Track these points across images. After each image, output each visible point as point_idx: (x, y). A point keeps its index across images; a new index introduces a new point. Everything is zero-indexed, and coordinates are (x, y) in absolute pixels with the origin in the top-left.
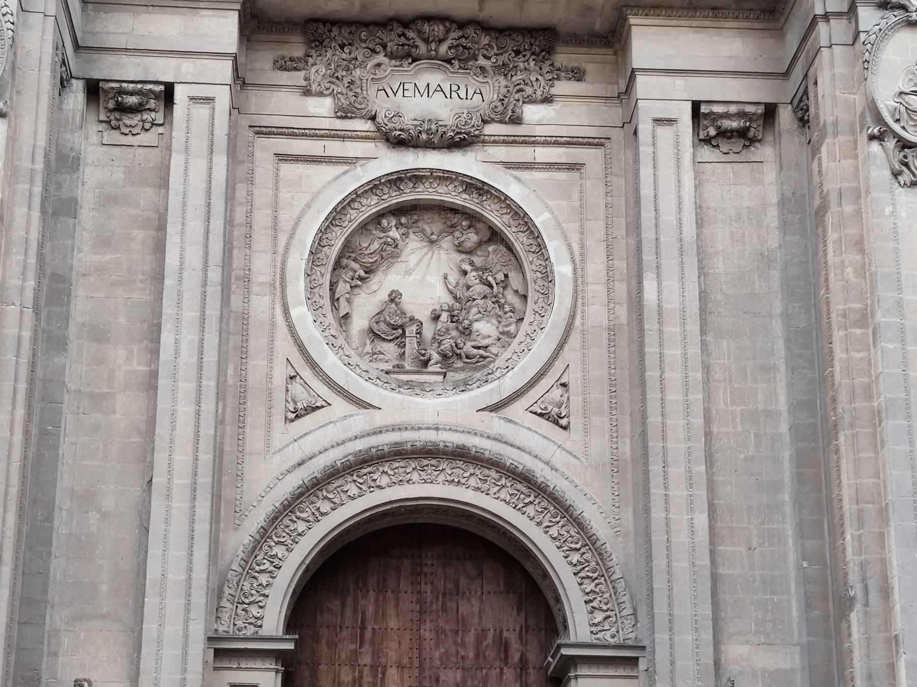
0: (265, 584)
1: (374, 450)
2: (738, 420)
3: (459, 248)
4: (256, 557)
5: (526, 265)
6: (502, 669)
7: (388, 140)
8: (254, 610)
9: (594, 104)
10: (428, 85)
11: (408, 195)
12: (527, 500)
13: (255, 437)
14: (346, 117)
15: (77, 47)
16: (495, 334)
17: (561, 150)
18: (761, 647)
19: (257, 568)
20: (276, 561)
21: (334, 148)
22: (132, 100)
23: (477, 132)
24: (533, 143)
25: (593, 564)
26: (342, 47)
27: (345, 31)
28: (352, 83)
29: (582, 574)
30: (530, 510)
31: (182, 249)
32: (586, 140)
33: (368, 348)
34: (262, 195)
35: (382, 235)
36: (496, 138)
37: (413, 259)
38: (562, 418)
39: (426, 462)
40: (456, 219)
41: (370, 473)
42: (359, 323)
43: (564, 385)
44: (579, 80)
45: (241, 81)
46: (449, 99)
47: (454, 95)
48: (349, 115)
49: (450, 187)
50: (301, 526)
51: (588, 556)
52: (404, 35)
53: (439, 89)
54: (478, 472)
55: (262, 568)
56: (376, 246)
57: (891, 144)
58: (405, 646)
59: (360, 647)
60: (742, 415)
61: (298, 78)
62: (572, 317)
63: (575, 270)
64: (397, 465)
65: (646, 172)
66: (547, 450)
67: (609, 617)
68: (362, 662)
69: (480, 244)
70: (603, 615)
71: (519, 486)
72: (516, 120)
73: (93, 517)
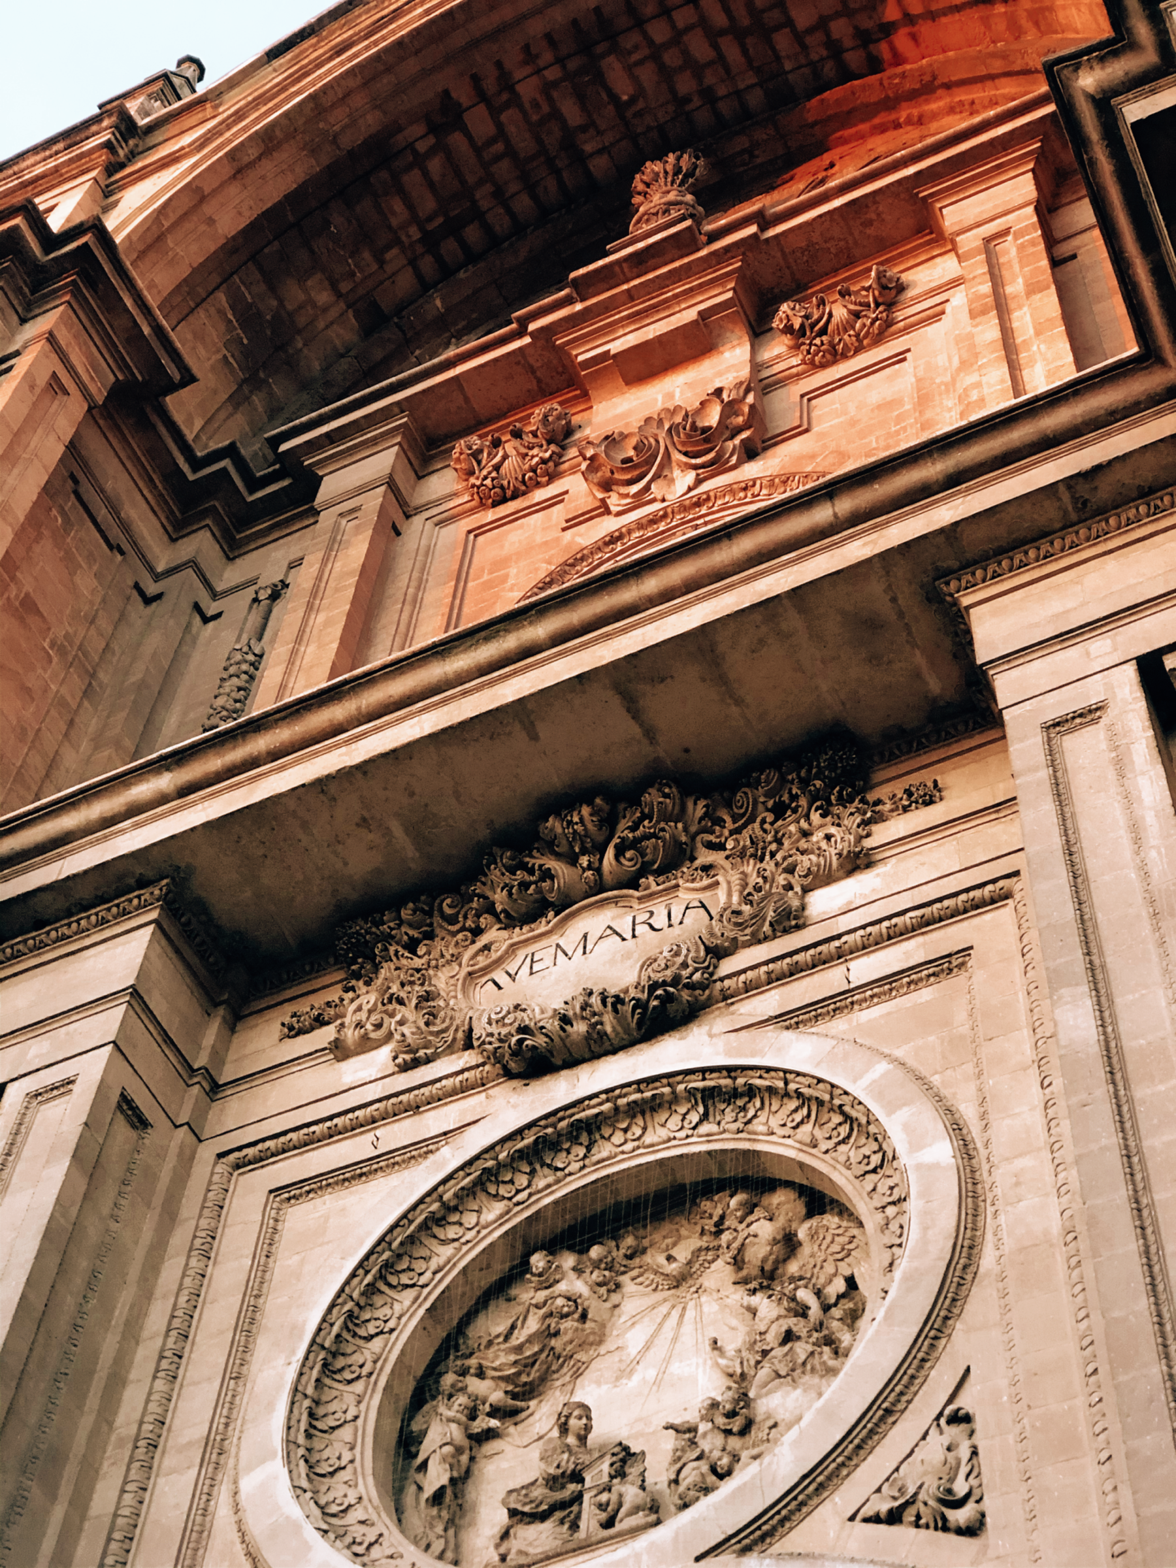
7: (509, 1075)
10: (585, 937)
14: (416, 1063)
23: (697, 976)
24: (841, 955)
28: (428, 997)
32: (963, 897)
35: (541, 1295)
36: (750, 974)
40: (713, 1207)
44: (929, 802)
46: (630, 942)
47: (640, 929)
48: (421, 1053)
49: (674, 1122)
52: (524, 867)
53: (609, 932)
56: (533, 1325)
61: (325, 1035)
69: (789, 1243)
72: (790, 920)
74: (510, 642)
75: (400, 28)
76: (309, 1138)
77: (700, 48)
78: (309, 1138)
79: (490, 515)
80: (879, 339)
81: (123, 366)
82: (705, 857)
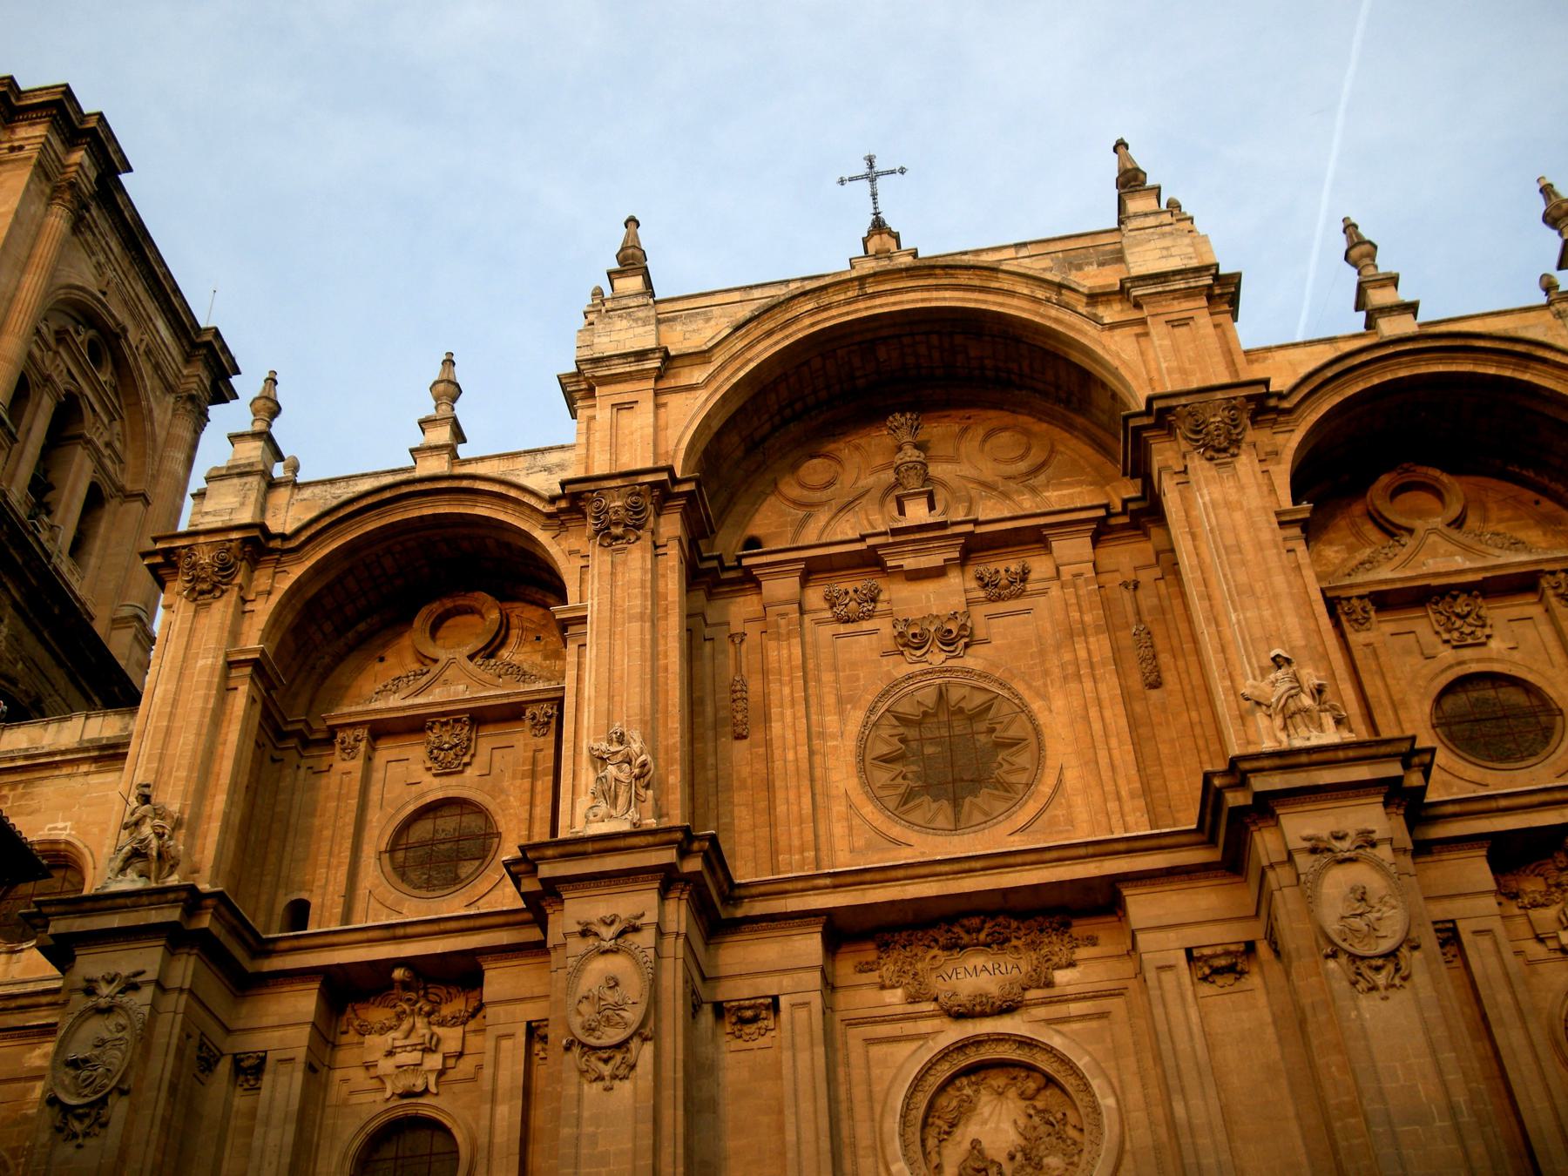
3: (1022, 1096)
5: (1078, 1103)
9: (1110, 963)
11: (974, 1057)
15: (704, 979)
17: (1089, 1003)
21: (909, 1028)
22: (749, 1013)
26: (904, 947)
27: (904, 935)
28: (915, 974)
31: (798, 1127)
34: (858, 1073)
37: (986, 1111)
40: (1015, 1072)
44: (1094, 945)
45: (830, 986)
56: (954, 1103)
57: (1343, 959)
61: (874, 977)
62: (1122, 1143)
63: (1118, 1101)
65: (1158, 1011)
69: (1039, 1090)
72: (1050, 984)
74: (966, 866)
75: (799, 330)
76: (873, 1021)
77: (923, 350)
78: (873, 1021)
79: (842, 628)
80: (1018, 596)
81: (692, 532)
82: (1014, 942)
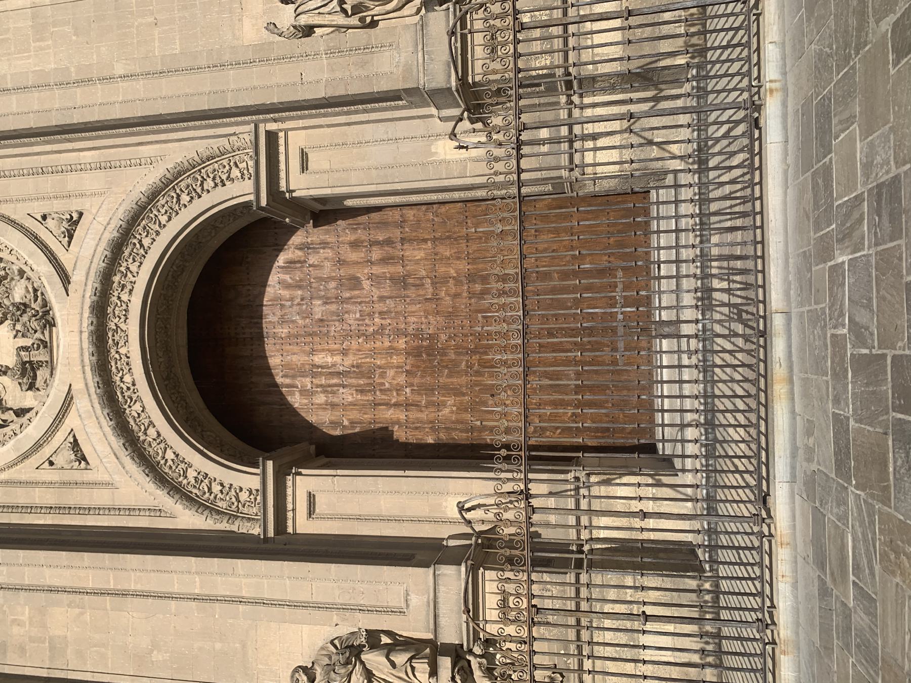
0: (220, 488)
1: (98, 391)
2: (42, 44)
4: (198, 496)
6: (310, 266)
8: (244, 496)
12: (138, 246)
13: (101, 497)
16: (23, 282)
18: (243, 6)
19: (207, 495)
20: (200, 477)
25: (189, 181)
29: (199, 190)
30: (146, 242)
33: (42, 392)
38: (72, 217)
39: (110, 341)
41: (122, 393)
42: (28, 399)
43: (44, 217)
50: (170, 455)
51: (183, 184)
54: (116, 294)
55: (206, 490)
58: (295, 348)
59: (297, 387)
60: (38, 40)
64: (114, 368)
66: (97, 227)
67: (236, 164)
68: (309, 386)
70: (234, 170)
71: (126, 253)
73: (157, 656)
